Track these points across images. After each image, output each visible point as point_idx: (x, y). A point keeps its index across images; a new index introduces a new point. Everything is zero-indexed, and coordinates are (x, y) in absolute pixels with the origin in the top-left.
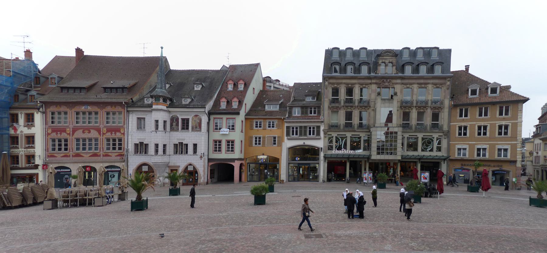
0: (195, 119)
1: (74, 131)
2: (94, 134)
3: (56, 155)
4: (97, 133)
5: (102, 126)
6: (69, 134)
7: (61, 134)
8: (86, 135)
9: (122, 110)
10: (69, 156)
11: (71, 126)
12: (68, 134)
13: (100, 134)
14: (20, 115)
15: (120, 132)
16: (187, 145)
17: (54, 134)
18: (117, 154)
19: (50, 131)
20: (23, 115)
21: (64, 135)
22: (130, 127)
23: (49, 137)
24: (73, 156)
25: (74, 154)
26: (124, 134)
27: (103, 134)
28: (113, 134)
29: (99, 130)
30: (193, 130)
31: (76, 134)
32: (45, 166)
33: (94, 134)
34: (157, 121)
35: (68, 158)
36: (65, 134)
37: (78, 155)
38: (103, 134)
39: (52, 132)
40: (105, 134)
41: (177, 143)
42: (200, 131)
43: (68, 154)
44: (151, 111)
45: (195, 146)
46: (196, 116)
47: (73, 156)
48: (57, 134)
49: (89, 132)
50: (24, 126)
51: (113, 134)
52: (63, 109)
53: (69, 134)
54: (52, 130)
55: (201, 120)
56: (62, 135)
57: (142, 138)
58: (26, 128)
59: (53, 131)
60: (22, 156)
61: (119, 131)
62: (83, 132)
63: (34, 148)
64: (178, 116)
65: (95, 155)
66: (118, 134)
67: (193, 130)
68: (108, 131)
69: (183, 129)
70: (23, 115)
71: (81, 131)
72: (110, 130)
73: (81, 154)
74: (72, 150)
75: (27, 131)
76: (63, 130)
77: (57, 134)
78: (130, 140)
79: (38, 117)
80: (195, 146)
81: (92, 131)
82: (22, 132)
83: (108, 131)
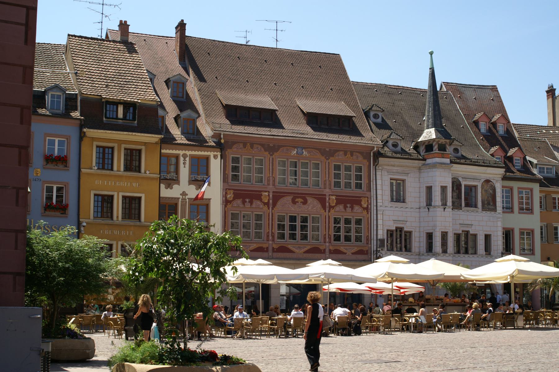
0: (485, 187)
1: (277, 197)
2: (312, 208)
4: (320, 206)
5: (327, 191)
6: (267, 204)
7: (251, 202)
8: (299, 210)
9: (365, 161)
10: (267, 250)
11: (271, 188)
12: (265, 204)
13: (324, 207)
14: (182, 159)
15: (361, 205)
16: (475, 236)
17: (239, 202)
18: (355, 249)
19: (230, 196)
20: (187, 159)
21: (258, 207)
22: (379, 197)
23: (229, 206)
24: (274, 250)
25: (275, 246)
26: (367, 209)
27: (331, 207)
28: (349, 210)
29: (322, 199)
30: (484, 209)
31: (279, 203)
34: (429, 189)
36: (259, 202)
38: (331, 207)
39: (234, 198)
40: (333, 207)
41: (461, 232)
42: (495, 210)
43: (265, 246)
44: (420, 169)
45: (487, 238)
46: (487, 181)
47: (274, 250)
48: (244, 202)
49: (305, 202)
50: (190, 184)
51: (349, 210)
53: (267, 204)
55: (494, 190)
56: (254, 205)
57: (400, 219)
58: (193, 187)
61: (359, 203)
62: (294, 202)
64: (460, 179)
66: (357, 208)
67: (484, 209)
69: (467, 205)
70: (187, 159)
71: (289, 198)
72: (342, 200)
73: (290, 247)
74: (273, 237)
76: (255, 196)
77: (244, 202)
78: (380, 222)
80: (487, 238)
81: (310, 200)
82: (184, 194)
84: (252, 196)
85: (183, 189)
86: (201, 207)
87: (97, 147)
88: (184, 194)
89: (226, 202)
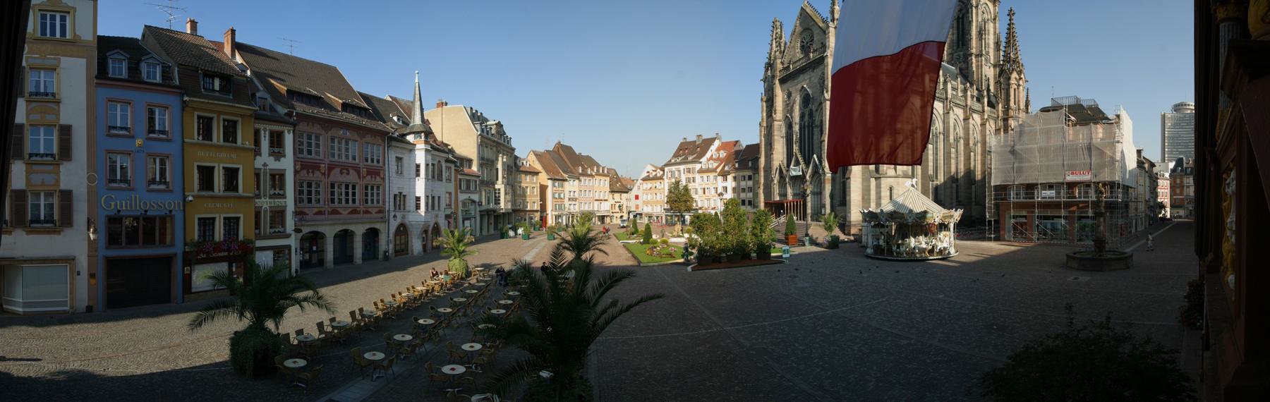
1: (331, 168)
3: (306, 210)
5: (362, 165)
17: (304, 172)
29: (358, 172)
32: (297, 231)
33: (352, 177)
35: (322, 217)
37: (335, 212)
52: (317, 129)
54: (304, 166)
58: (272, 158)
59: (303, 168)
60: (265, 212)
63: (284, 196)
65: (354, 211)
68: (369, 173)
75: (273, 164)
79: (289, 139)
82: (265, 165)
83: (369, 173)
84: (314, 167)
85: (265, 160)
86: (277, 178)
87: (199, 117)
88: (265, 165)
89: (296, 172)
